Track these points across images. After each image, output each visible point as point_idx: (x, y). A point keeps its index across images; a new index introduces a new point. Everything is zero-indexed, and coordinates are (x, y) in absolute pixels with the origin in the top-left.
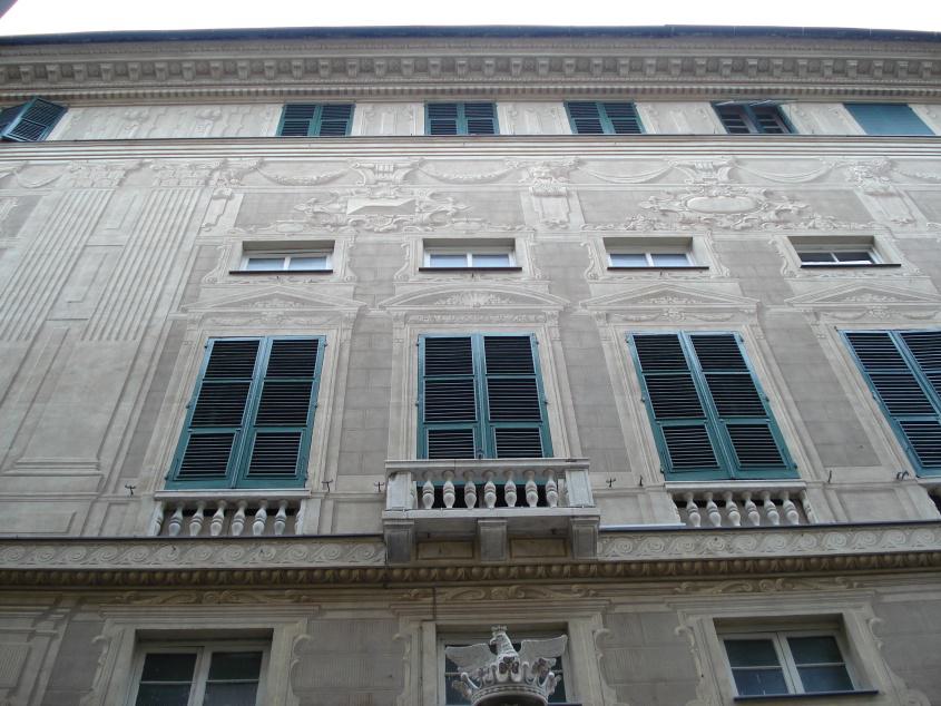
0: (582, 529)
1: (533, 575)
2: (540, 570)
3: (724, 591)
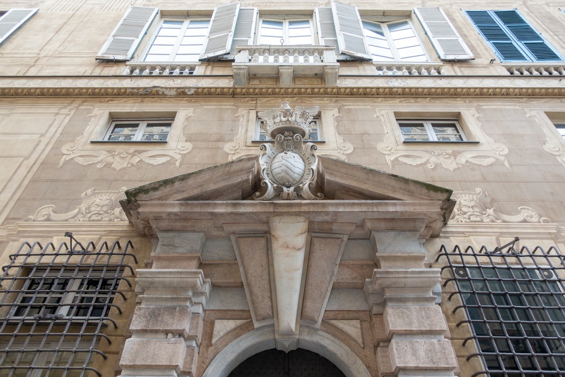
0: (329, 71)
1: (305, 93)
2: (309, 90)
3: (400, 102)
